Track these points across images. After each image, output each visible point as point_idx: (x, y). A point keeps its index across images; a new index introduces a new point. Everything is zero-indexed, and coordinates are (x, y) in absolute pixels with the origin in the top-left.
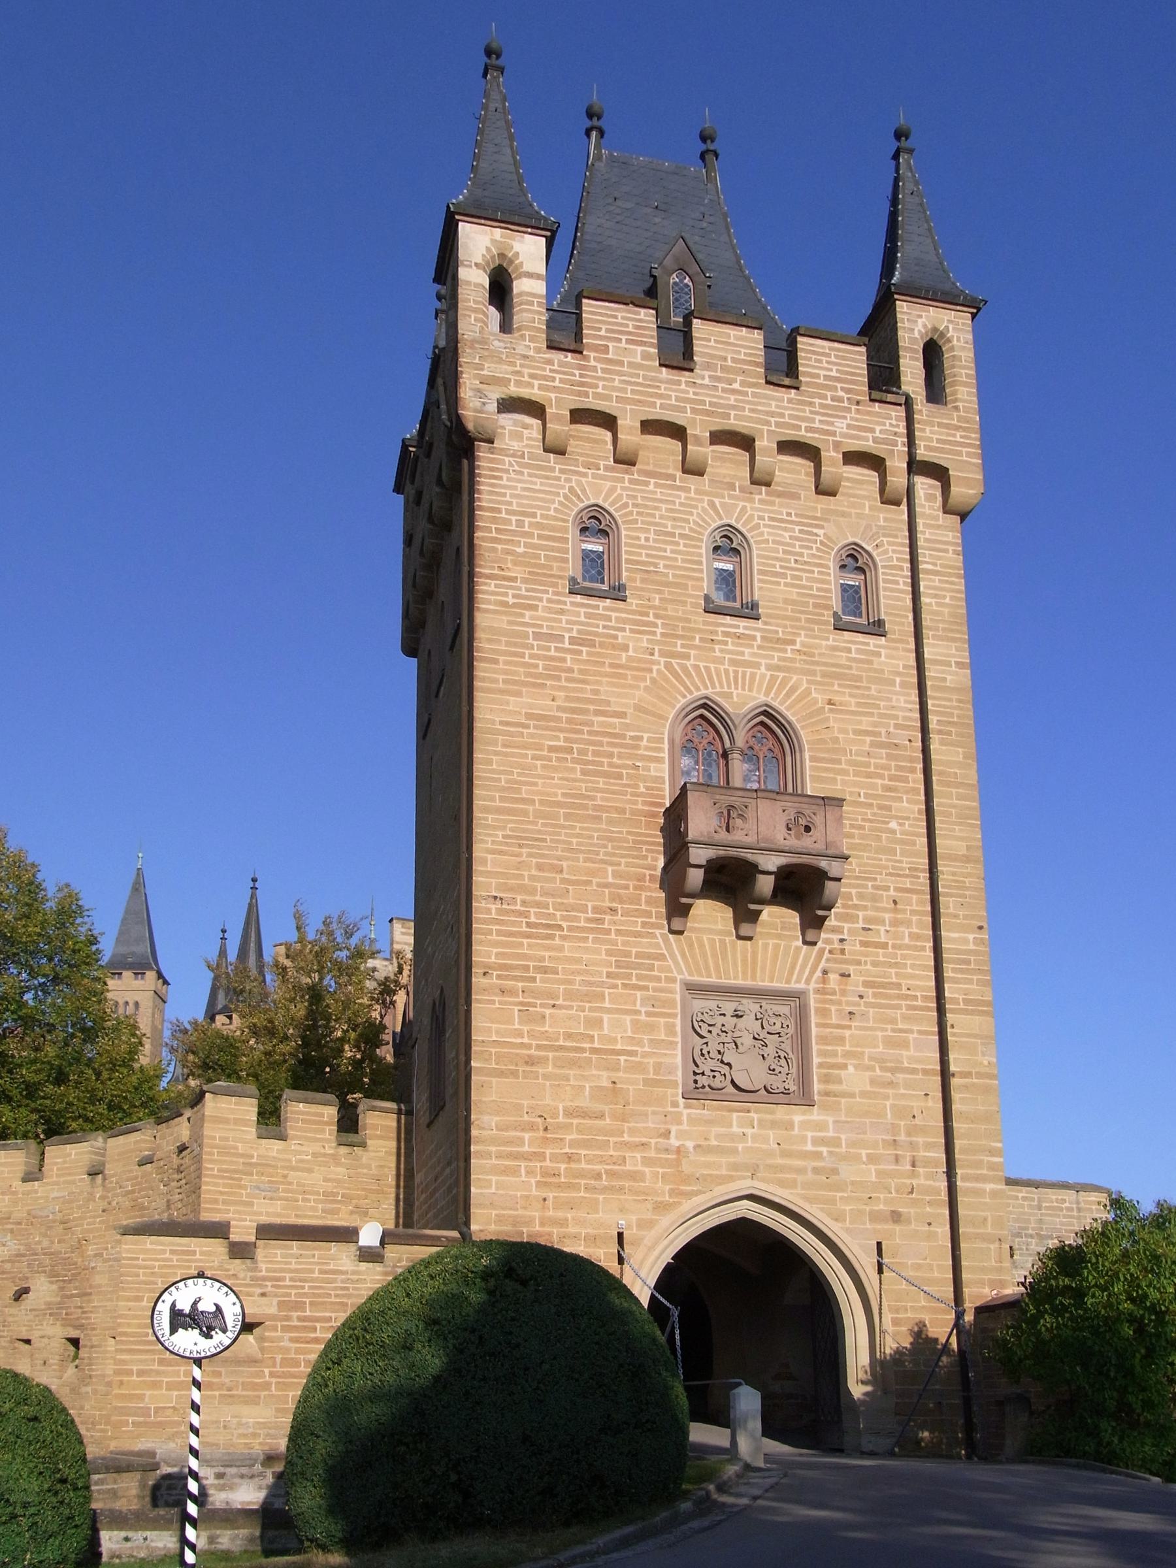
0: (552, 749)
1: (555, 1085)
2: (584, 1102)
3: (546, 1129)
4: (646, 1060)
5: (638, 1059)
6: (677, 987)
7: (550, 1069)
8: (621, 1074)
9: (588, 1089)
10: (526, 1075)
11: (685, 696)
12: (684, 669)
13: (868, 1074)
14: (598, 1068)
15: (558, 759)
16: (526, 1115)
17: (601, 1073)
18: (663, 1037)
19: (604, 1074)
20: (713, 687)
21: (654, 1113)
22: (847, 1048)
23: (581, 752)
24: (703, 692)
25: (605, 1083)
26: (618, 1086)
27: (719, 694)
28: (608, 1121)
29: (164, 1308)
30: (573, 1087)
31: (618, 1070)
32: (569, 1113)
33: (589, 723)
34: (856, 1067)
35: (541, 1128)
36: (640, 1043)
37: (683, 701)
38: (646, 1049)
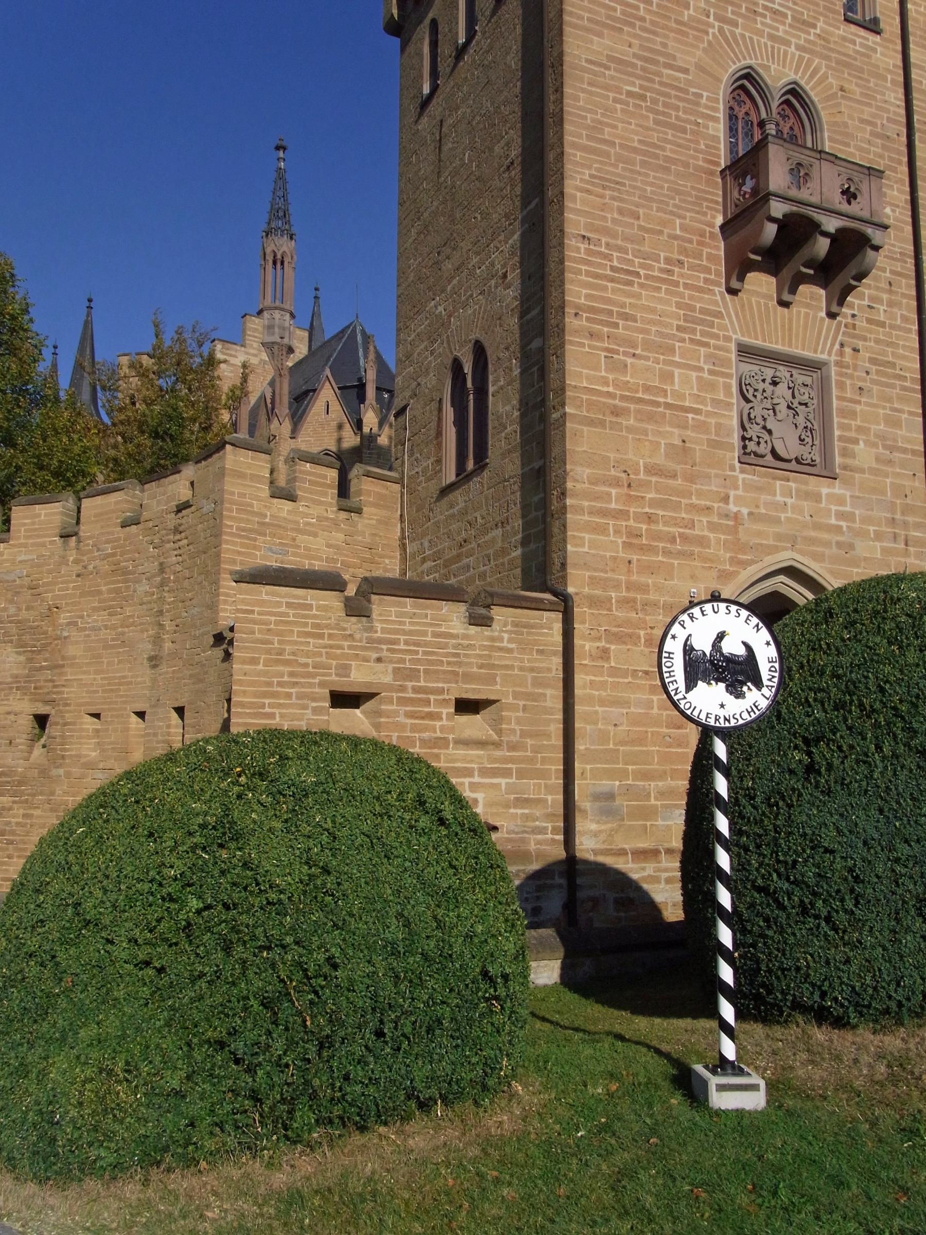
0: (630, 94)
2: (660, 459)
3: (629, 486)
5: (702, 418)
7: (632, 422)
8: (689, 433)
10: (613, 426)
11: (734, 63)
12: (733, 34)
13: (874, 450)
14: (671, 425)
15: (635, 105)
19: (676, 431)
20: (756, 59)
21: (716, 476)
22: (858, 423)
23: (654, 101)
24: (748, 62)
25: (677, 442)
26: (688, 445)
27: (760, 65)
28: (680, 481)
29: (674, 647)
30: (651, 442)
32: (651, 470)
33: (659, 74)
34: (865, 442)
36: (703, 401)
37: (734, 67)
38: (709, 408)
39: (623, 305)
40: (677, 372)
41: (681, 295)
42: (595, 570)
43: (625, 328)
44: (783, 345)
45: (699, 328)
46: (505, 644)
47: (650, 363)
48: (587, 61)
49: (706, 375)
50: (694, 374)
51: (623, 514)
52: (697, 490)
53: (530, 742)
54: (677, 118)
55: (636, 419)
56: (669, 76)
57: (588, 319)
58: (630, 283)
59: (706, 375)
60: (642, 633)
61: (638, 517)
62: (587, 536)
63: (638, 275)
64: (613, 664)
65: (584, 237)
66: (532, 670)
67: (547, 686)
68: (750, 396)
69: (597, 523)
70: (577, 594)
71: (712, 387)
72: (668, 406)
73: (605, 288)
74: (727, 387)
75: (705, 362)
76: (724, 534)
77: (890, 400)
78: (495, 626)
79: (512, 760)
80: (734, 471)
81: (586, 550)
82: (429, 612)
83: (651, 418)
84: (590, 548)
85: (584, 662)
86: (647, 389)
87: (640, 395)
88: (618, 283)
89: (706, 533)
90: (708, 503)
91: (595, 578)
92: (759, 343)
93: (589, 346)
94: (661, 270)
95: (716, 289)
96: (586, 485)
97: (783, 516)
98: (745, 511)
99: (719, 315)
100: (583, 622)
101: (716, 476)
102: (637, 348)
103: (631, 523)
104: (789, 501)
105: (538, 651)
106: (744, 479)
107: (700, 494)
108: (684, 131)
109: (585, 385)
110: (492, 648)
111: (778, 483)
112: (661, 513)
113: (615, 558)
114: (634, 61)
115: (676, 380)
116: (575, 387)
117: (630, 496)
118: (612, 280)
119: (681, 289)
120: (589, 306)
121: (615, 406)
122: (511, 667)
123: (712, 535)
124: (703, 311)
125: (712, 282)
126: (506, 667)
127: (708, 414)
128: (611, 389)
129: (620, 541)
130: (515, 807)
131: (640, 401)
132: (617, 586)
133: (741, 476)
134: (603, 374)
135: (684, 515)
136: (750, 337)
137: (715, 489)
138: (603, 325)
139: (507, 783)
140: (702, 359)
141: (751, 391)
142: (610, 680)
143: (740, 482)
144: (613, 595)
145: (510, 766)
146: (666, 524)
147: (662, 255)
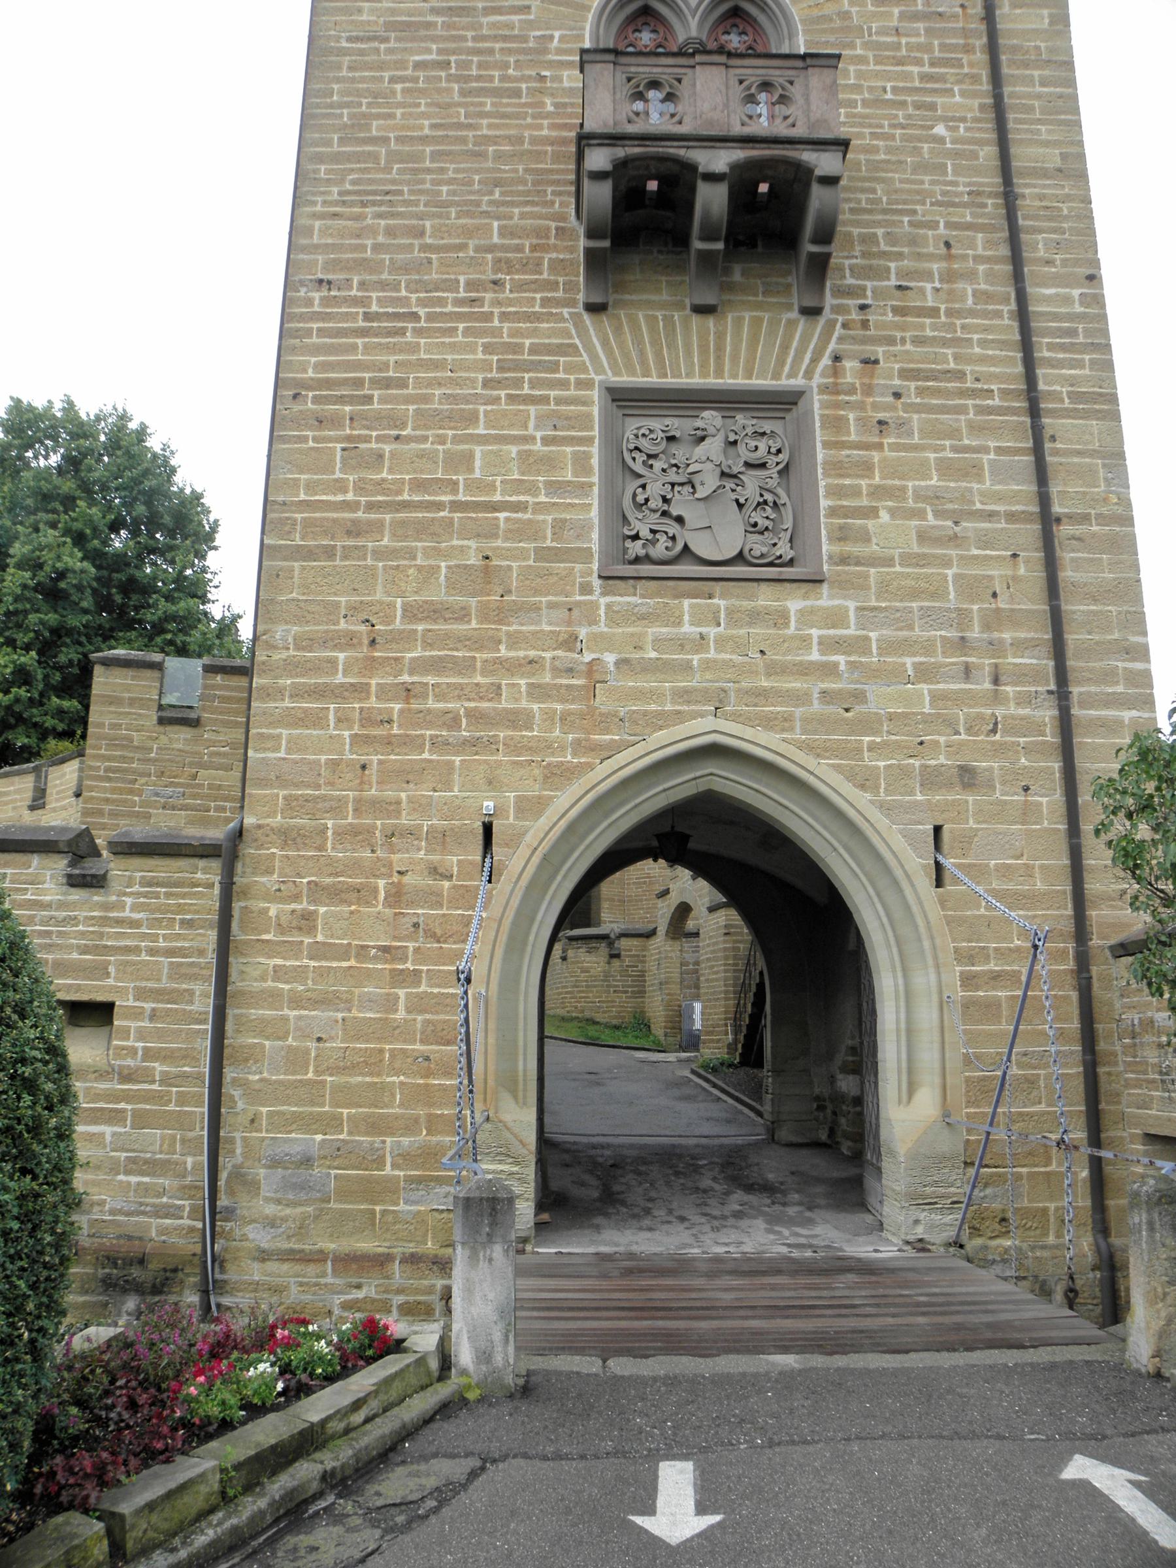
1: (391, 567)
2: (438, 594)
3: (373, 642)
4: (541, 517)
6: (595, 394)
8: (499, 543)
9: (444, 571)
16: (342, 621)
17: (466, 542)
18: (569, 478)
19: (472, 544)
25: (473, 560)
30: (420, 569)
31: (495, 536)
32: (411, 613)
35: (366, 642)
36: (532, 489)
39: (385, 366)
40: (478, 450)
41: (497, 332)
42: (297, 786)
43: (382, 400)
44: (704, 375)
45: (526, 376)
46: (127, 913)
47: (428, 446)
48: (349, 39)
49: (538, 447)
50: (514, 450)
51: (360, 690)
52: (508, 634)
53: (159, 1067)
54: (504, 78)
55: (394, 535)
56: (493, 25)
57: (316, 399)
58: (402, 332)
59: (538, 447)
60: (381, 883)
61: (384, 692)
62: (285, 732)
63: (415, 316)
64: (320, 938)
65: (321, 281)
66: (170, 952)
67: (194, 978)
68: (638, 467)
69: (305, 710)
70: (259, 827)
71: (549, 463)
72: (456, 506)
73: (354, 347)
74: (582, 462)
75: (537, 427)
76: (563, 701)
77: (954, 433)
78: (115, 885)
79: (127, 1097)
80: (591, 592)
81: (282, 754)
82: (9, 871)
83: (422, 529)
84: (289, 750)
85: (265, 937)
86: (419, 485)
87: (406, 497)
88: (376, 336)
89: (524, 704)
90: (532, 653)
91: (297, 798)
92: (653, 380)
93: (315, 439)
94: (459, 302)
95: (565, 312)
96: (292, 652)
97: (696, 659)
98: (610, 658)
99: (562, 350)
100: (269, 872)
101: (552, 606)
102: (404, 426)
103: (373, 702)
104: (712, 632)
105: (182, 922)
106: (609, 606)
107: (515, 641)
108: (517, 93)
109: (302, 497)
110: (104, 922)
111: (686, 603)
112: (431, 680)
113: (334, 764)
114: (429, 18)
115: (478, 463)
116: (284, 504)
117: (374, 659)
118: (364, 333)
119: (496, 323)
120: (319, 379)
121: (354, 522)
122: (136, 950)
123: (535, 707)
124: (534, 350)
125: (558, 303)
126: (128, 950)
127: (539, 508)
128: (350, 496)
129: (346, 733)
130: (127, 1172)
131: (406, 505)
132: (337, 809)
133: (603, 601)
134: (338, 475)
135: (479, 679)
136: (634, 374)
137: (548, 628)
138: (344, 403)
139: (114, 1134)
140: (531, 424)
141: (640, 458)
142: (313, 963)
143: (602, 612)
144: (330, 824)
145: (122, 1105)
146: (440, 697)
147: (462, 279)
